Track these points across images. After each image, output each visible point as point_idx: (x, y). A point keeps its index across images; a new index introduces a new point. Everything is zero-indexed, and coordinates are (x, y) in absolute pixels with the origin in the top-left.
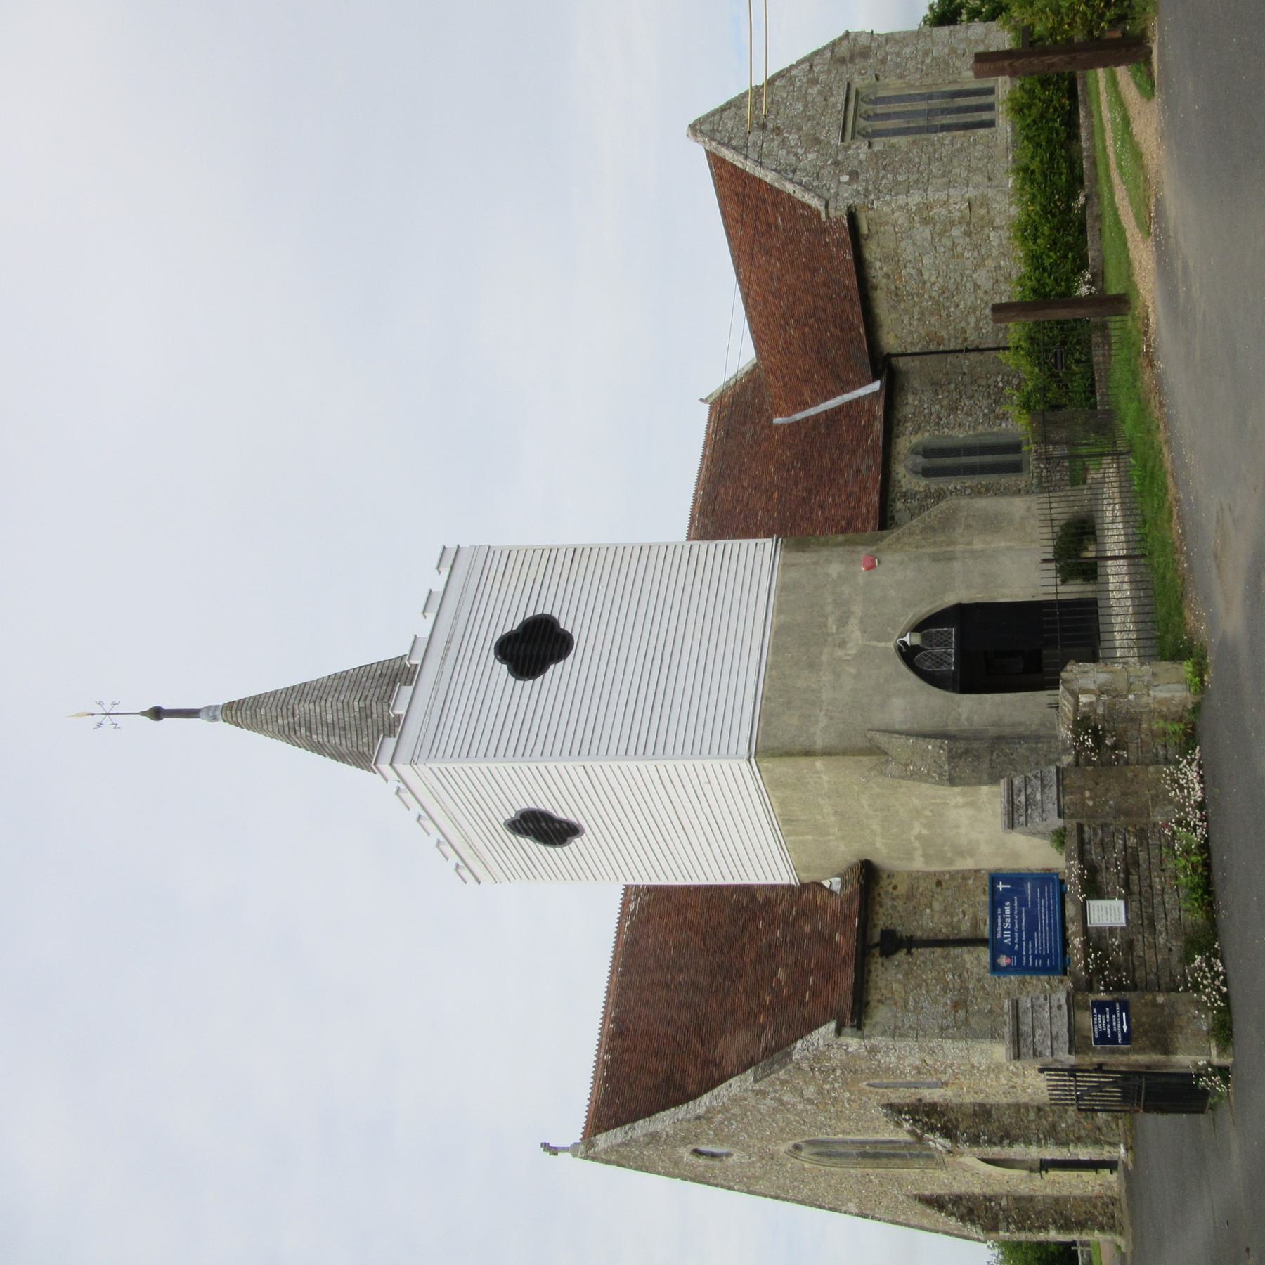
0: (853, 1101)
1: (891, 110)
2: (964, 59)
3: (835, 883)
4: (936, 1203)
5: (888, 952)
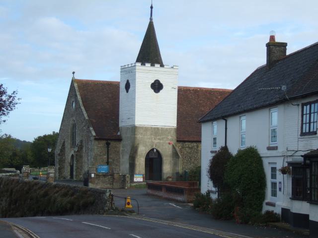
3: (119, 134)
5: (106, 143)
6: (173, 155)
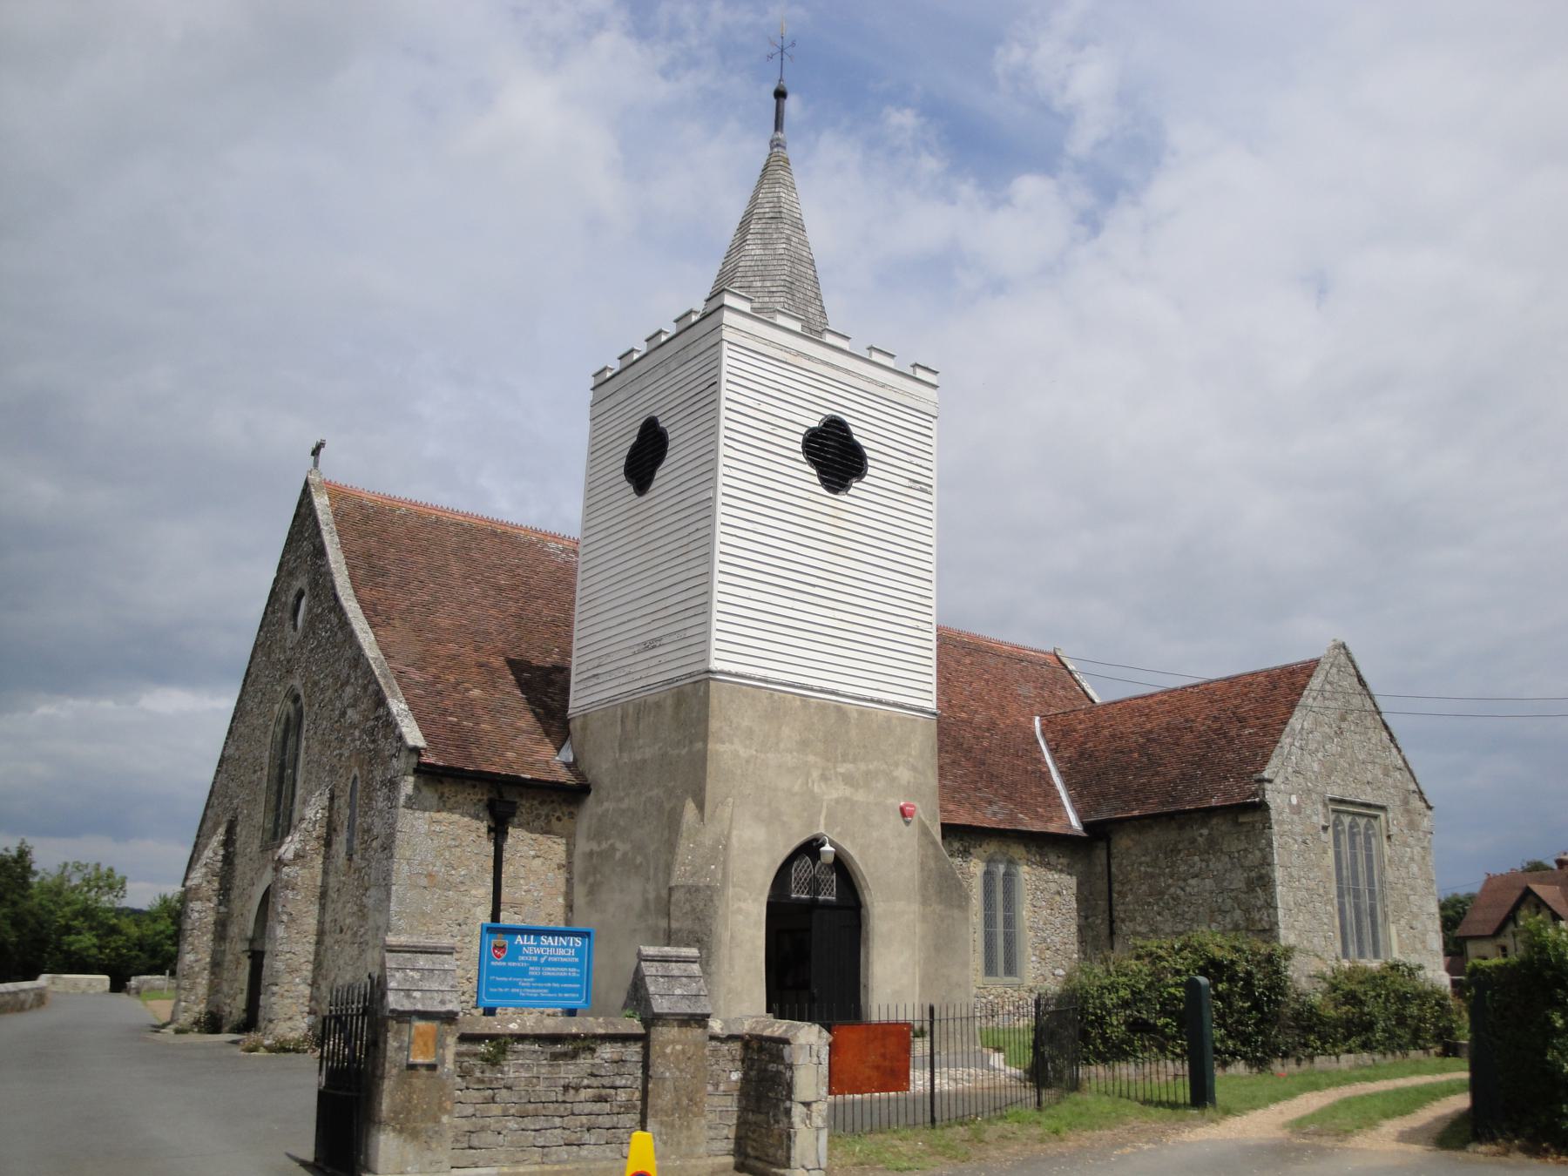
0: (340, 760)
1: (1358, 851)
2: (1408, 928)
6: (924, 886)
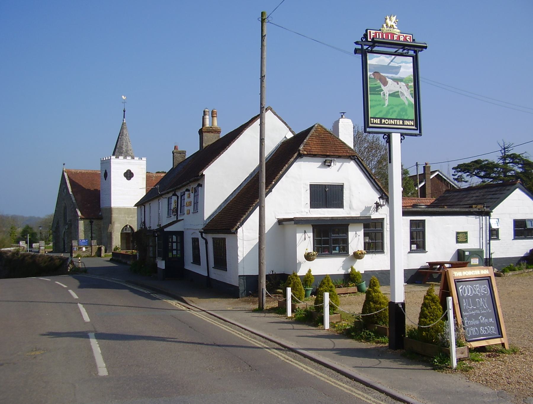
3: (100, 214)
4: (58, 223)
5: (90, 222)
